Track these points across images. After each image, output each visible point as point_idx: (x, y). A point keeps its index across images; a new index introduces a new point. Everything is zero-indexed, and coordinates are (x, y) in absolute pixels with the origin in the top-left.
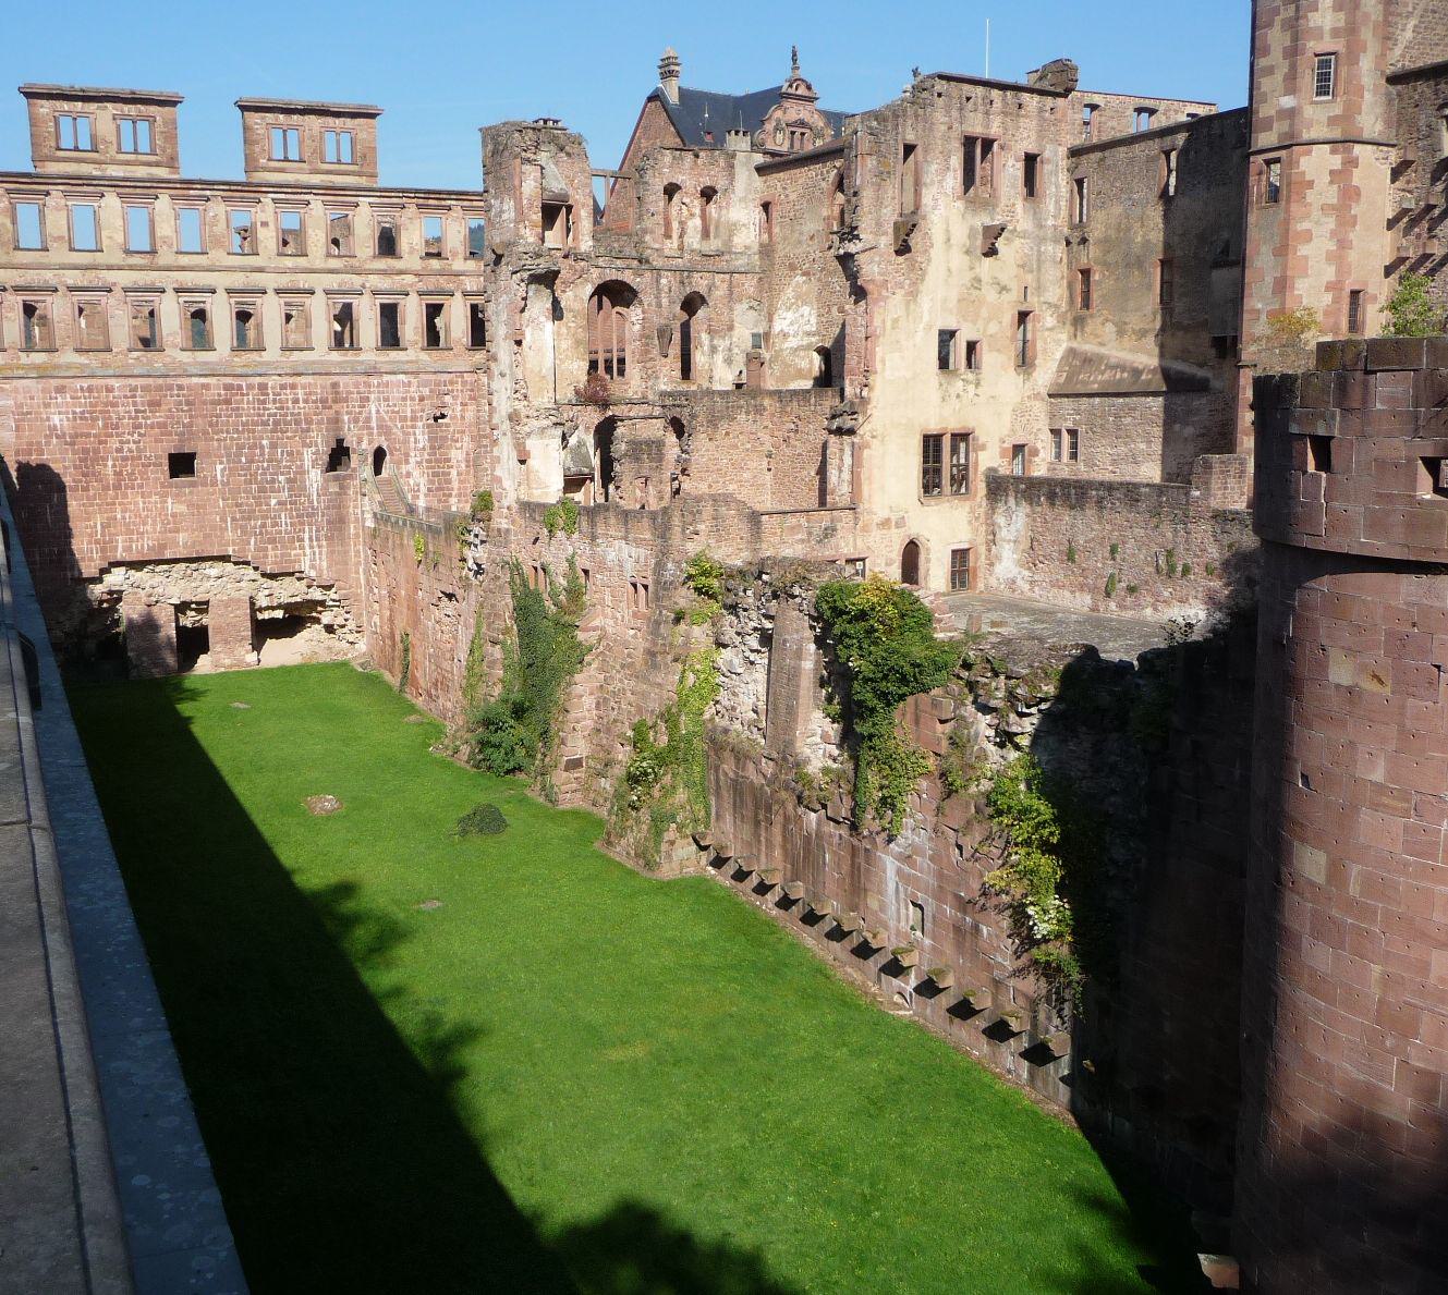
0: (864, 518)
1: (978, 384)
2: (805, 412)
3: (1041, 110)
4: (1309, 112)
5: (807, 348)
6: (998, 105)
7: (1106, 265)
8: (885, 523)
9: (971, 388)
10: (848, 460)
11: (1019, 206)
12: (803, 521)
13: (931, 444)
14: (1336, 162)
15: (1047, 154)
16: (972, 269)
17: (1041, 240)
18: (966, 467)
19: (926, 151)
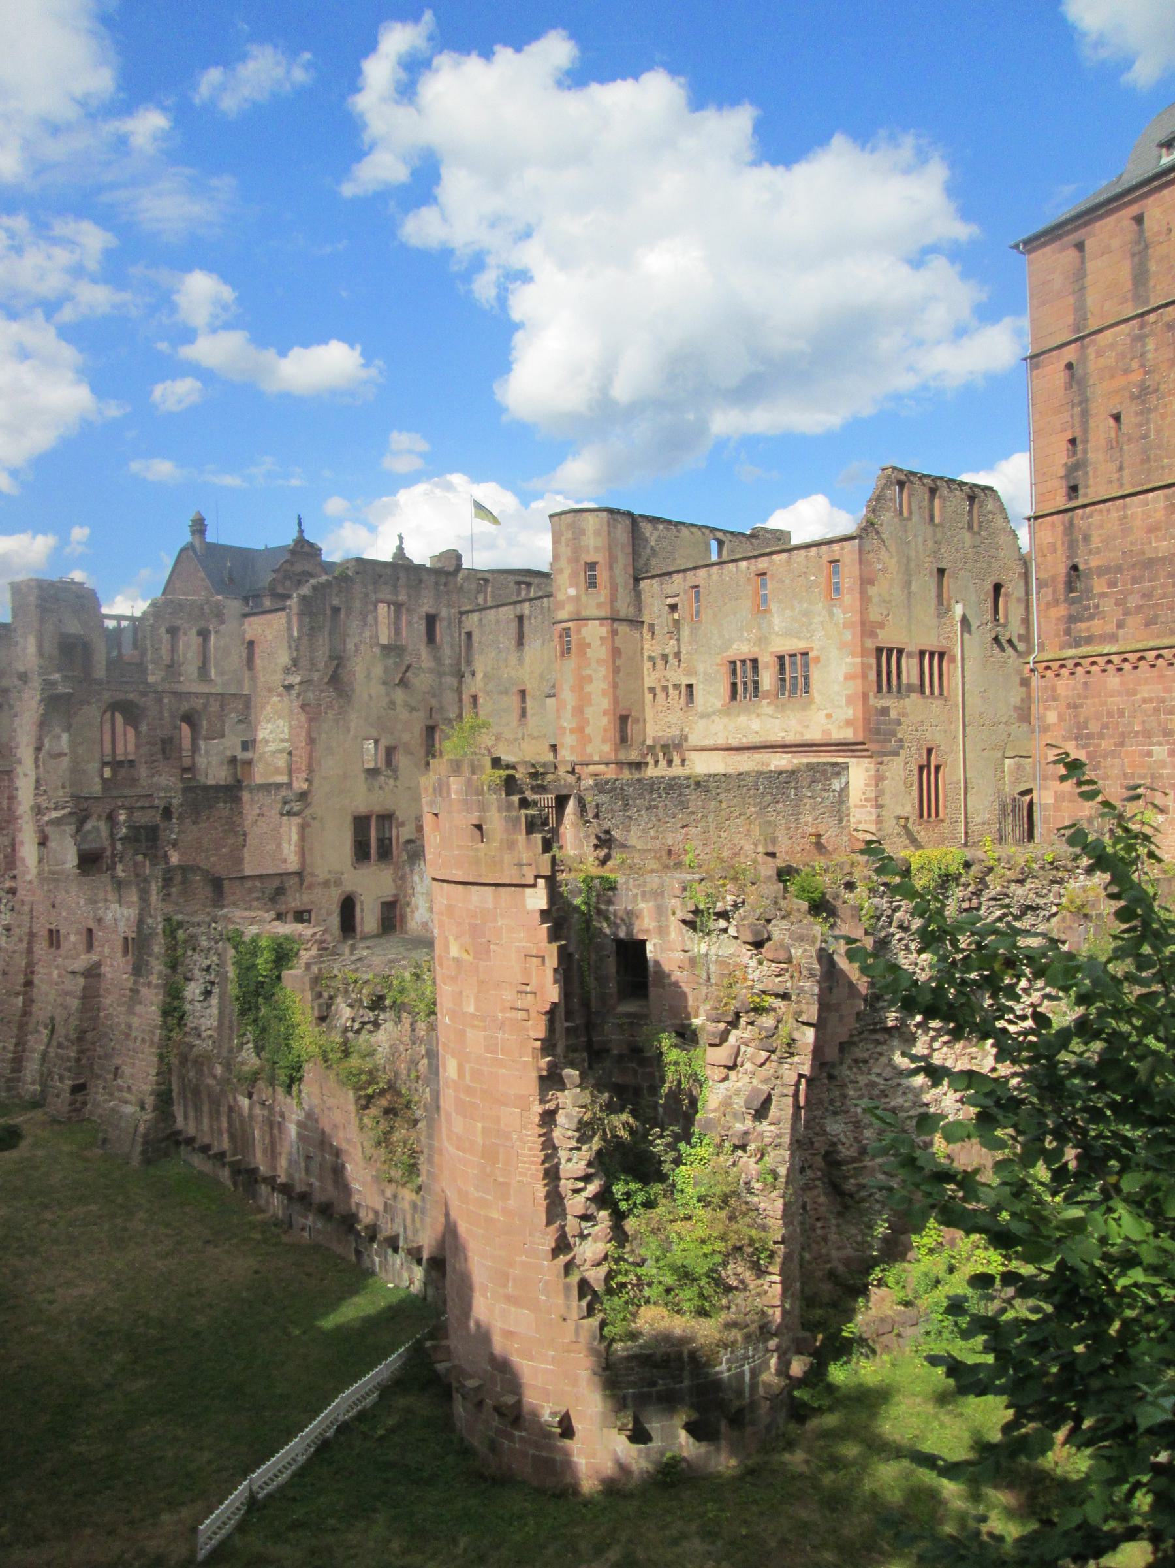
0: (308, 880)
1: (396, 779)
2: (268, 800)
3: (436, 584)
4: (584, 599)
5: (281, 751)
6: (403, 581)
7: (487, 693)
8: (326, 884)
9: (391, 782)
10: (295, 837)
11: (424, 651)
12: (258, 884)
13: (361, 823)
14: (604, 631)
15: (444, 613)
16: (388, 694)
17: (440, 674)
18: (390, 839)
19: (348, 615)
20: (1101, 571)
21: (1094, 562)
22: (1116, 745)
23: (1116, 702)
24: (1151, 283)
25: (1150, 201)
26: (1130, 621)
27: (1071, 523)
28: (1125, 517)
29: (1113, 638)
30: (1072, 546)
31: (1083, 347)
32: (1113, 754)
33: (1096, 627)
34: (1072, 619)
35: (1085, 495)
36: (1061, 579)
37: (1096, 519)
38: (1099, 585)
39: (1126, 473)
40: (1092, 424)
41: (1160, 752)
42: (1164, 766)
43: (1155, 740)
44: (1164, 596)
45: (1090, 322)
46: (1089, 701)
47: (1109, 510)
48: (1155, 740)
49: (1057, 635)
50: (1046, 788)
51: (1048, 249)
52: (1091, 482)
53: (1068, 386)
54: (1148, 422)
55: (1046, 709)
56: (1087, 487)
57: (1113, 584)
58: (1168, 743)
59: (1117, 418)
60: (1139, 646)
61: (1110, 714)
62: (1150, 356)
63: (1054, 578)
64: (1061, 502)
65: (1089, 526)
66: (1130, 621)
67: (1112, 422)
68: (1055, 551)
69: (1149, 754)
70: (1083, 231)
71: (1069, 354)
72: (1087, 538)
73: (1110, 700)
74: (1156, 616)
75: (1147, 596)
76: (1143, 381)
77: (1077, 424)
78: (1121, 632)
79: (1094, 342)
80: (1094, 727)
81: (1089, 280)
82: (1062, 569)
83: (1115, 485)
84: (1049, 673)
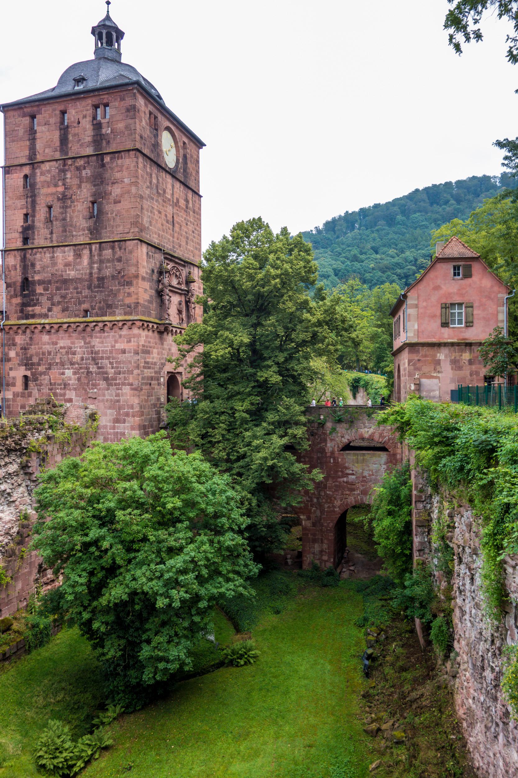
20: (40, 282)
21: (37, 278)
22: (46, 369)
23: (47, 348)
24: (70, 145)
26: (55, 308)
28: (53, 257)
29: (46, 316)
30: (25, 268)
32: (44, 373)
33: (37, 310)
34: (24, 305)
35: (33, 243)
36: (19, 284)
37: (38, 256)
38: (39, 289)
39: (54, 235)
40: (37, 209)
41: (69, 373)
42: (70, 380)
43: (66, 367)
44: (72, 298)
45: (38, 156)
46: (33, 347)
47: (45, 253)
48: (66, 367)
49: (16, 312)
50: (8, 390)
51: (16, 113)
52: (36, 237)
53: (25, 186)
54: (66, 213)
55: (9, 350)
56: (34, 239)
57: (46, 289)
58: (72, 368)
59: (50, 207)
60: (59, 321)
61: (43, 354)
62: (68, 181)
63: (15, 283)
64: (19, 244)
65: (35, 259)
66: (55, 308)
67: (47, 209)
68: (16, 269)
69: (63, 374)
70: (35, 109)
71: (27, 170)
72: (33, 265)
73: (44, 347)
74: (68, 307)
75: (64, 297)
76: (64, 192)
78: (50, 313)
79: (40, 167)
80: (35, 360)
81: (38, 135)
82: (19, 279)
83: (49, 241)
84: (11, 332)
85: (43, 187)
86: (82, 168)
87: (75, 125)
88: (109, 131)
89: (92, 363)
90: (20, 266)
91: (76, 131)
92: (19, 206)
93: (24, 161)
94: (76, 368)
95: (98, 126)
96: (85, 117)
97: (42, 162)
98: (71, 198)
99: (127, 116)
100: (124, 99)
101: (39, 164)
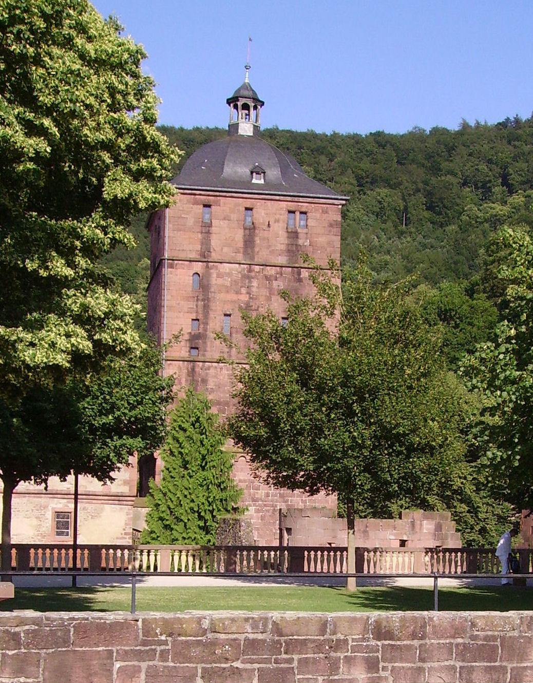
24: (256, 249)
25: (259, 203)
27: (193, 369)
31: (207, 267)
35: (204, 355)
37: (212, 371)
40: (212, 315)
45: (213, 254)
47: (221, 369)
52: (208, 349)
58: (254, 505)
62: (254, 289)
65: (207, 374)
71: (198, 267)
72: (204, 381)
77: (200, 311)
81: (213, 229)
85: (220, 292)
86: (272, 278)
87: (265, 227)
88: (307, 243)
89: (281, 500)
90: (186, 380)
91: (266, 234)
92: (186, 310)
93: (193, 256)
94: (259, 505)
95: (293, 235)
96: (277, 221)
97: (221, 263)
98: (257, 310)
99: (330, 231)
100: (327, 212)
101: (215, 264)
